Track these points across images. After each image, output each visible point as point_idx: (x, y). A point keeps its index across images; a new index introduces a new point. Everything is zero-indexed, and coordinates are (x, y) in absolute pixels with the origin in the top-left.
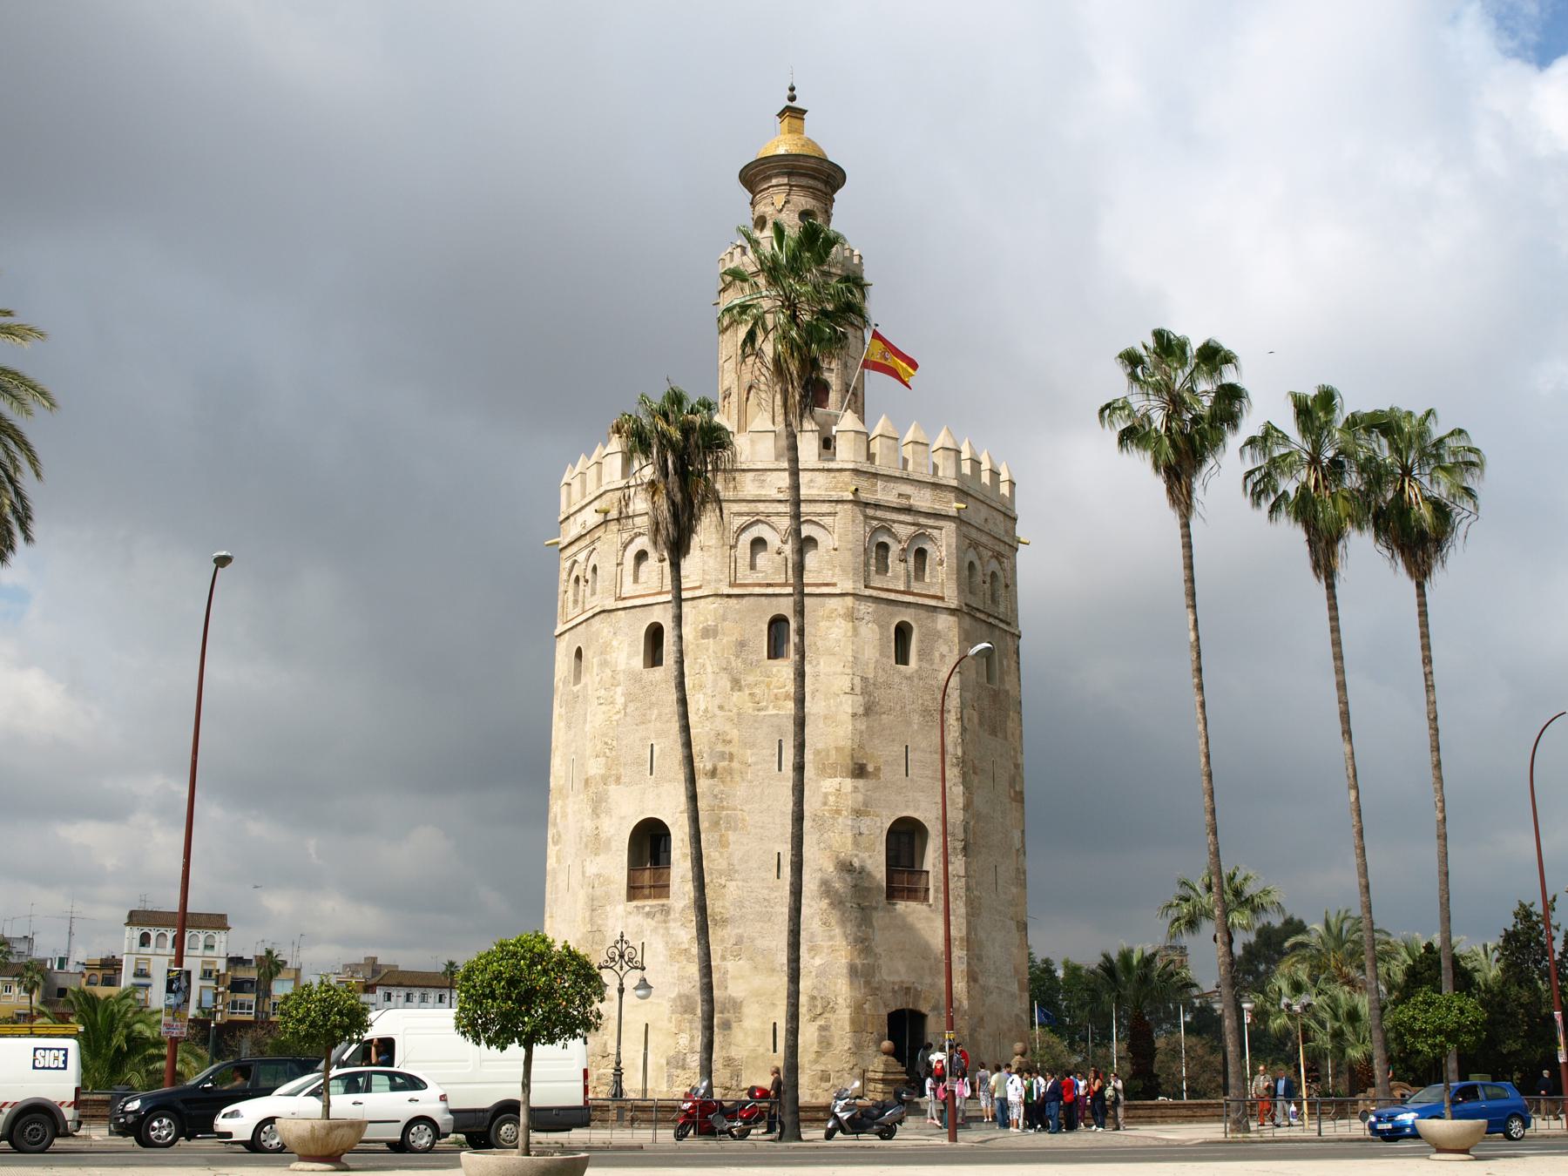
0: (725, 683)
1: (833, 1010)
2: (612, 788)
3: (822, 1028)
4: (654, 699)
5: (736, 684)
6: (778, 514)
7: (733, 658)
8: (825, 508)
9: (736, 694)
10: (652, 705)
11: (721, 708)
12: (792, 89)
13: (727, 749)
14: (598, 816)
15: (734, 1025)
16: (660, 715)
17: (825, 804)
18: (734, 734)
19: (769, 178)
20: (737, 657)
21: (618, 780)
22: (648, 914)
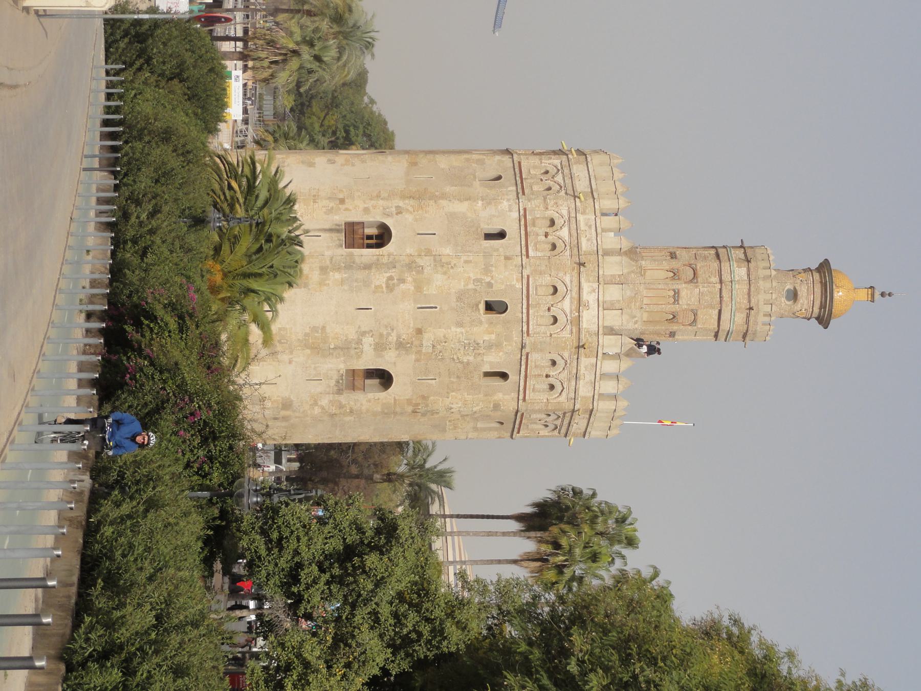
6: (563, 421)
10: (458, 377)
12: (890, 295)
14: (396, 349)
16: (453, 383)
19: (820, 309)
21: (417, 360)
22: (338, 382)
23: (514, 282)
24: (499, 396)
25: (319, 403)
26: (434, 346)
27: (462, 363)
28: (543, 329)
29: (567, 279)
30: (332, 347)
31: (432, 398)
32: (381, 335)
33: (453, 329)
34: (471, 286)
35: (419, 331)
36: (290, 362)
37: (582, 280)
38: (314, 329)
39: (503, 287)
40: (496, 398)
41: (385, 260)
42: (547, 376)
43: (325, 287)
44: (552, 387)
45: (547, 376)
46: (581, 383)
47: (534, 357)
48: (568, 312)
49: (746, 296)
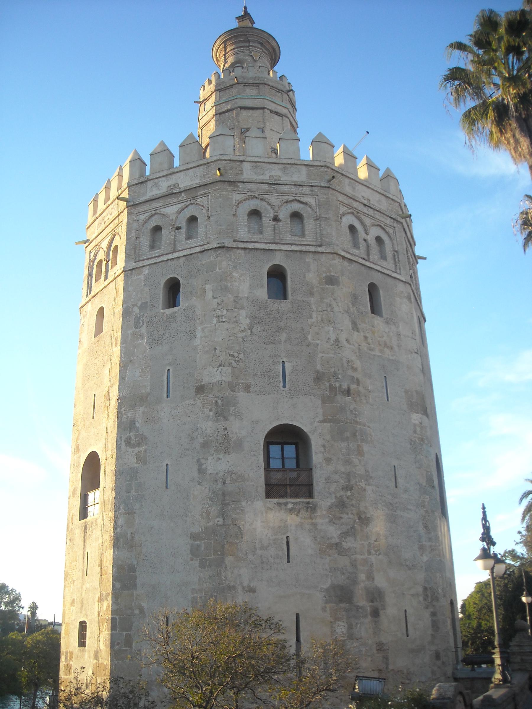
0: (347, 323)
1: (437, 599)
2: (241, 395)
3: (434, 614)
4: (282, 324)
5: (355, 327)
7: (351, 306)
8: (389, 221)
9: (356, 333)
10: (279, 330)
11: (347, 341)
13: (355, 375)
14: (226, 419)
15: (381, 612)
17: (415, 432)
18: (358, 364)
20: (353, 305)
21: (247, 388)
22: (291, 511)
23: (142, 277)
24: (312, 277)
25: (336, 540)
26: (220, 366)
27: (251, 327)
28: (201, 230)
29: (142, 217)
30: (221, 521)
31: (319, 367)
32: (205, 445)
33: (197, 342)
34: (144, 330)
35: (200, 389)
36: (252, 590)
37: (143, 199)
38: (194, 552)
39: (147, 289)
40: (315, 281)
41: (109, 454)
42: (276, 219)
43: (136, 538)
44: (296, 216)
45: (276, 219)
46: (284, 179)
47: (243, 233)
48: (179, 206)
49: (227, 91)
